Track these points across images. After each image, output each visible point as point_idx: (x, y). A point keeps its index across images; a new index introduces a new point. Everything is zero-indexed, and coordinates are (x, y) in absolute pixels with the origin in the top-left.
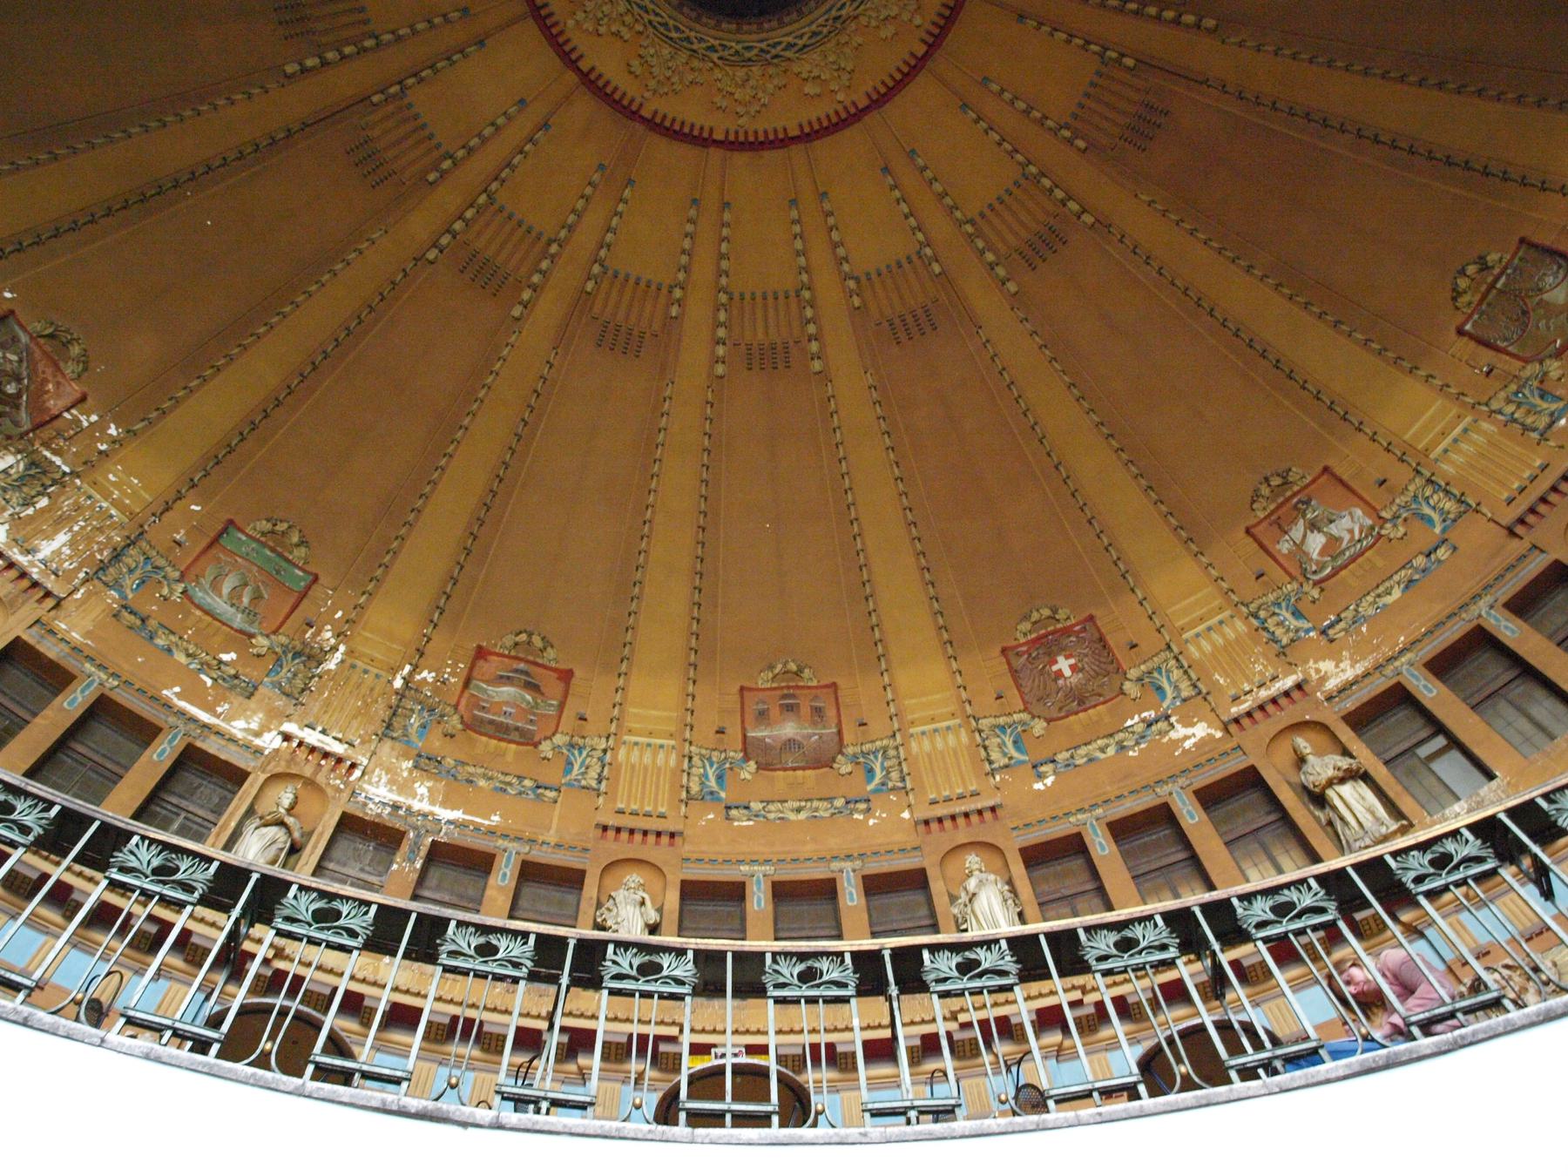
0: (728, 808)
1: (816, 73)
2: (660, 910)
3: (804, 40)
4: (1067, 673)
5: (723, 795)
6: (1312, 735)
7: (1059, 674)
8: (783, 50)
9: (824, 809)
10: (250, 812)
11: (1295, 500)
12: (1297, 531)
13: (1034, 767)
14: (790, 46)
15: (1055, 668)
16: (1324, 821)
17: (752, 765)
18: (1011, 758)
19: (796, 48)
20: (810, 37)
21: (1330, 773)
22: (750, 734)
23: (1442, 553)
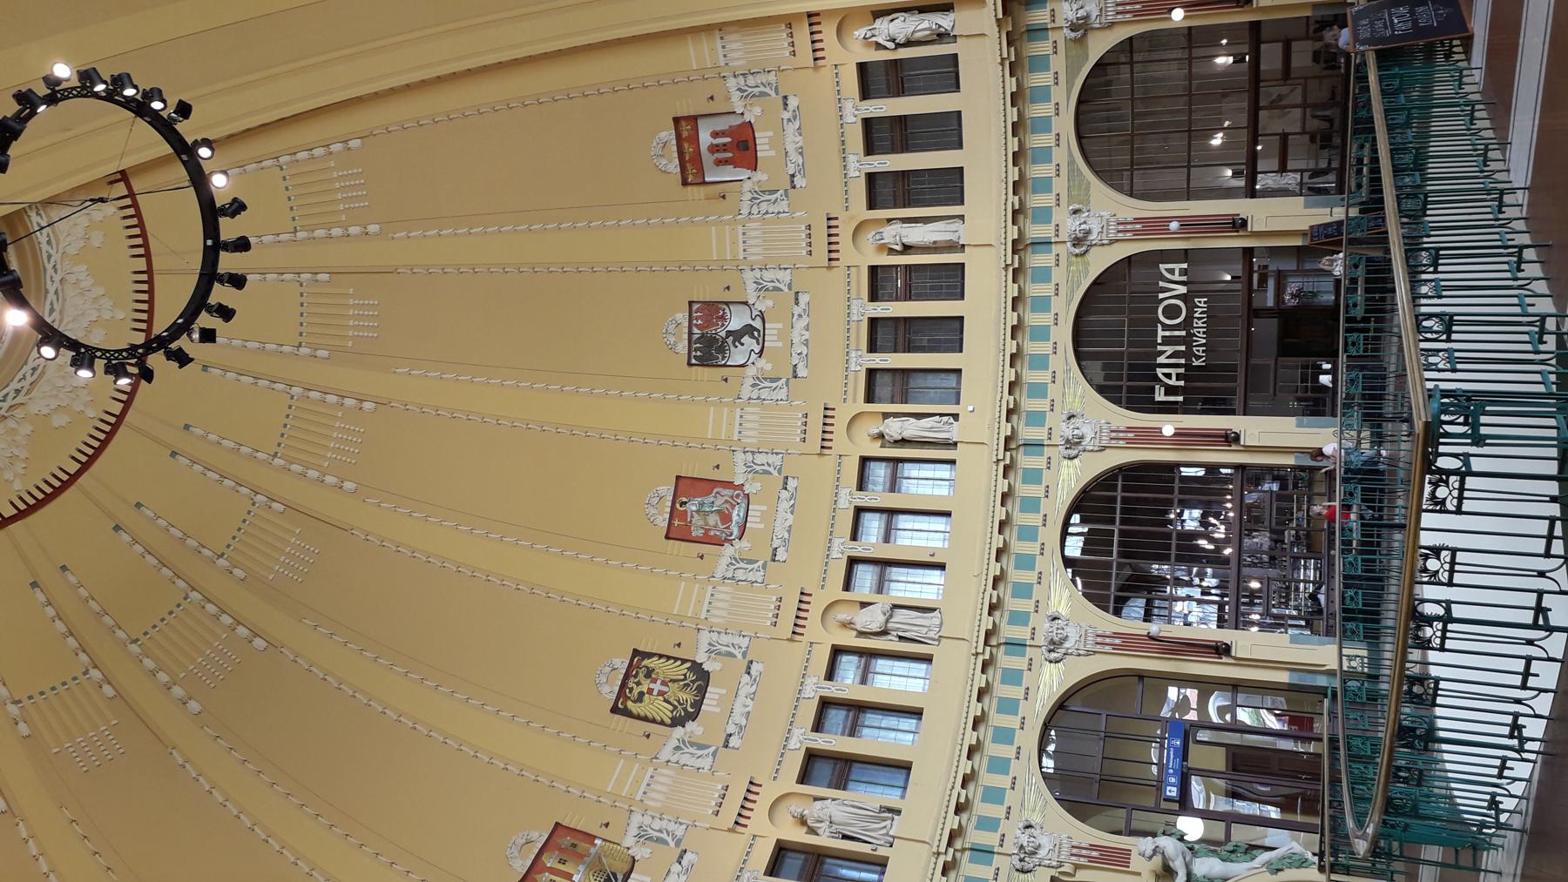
1: (54, 404)
3: (29, 379)
4: (664, 689)
6: (838, 608)
7: (661, 693)
8: (14, 398)
11: (678, 506)
12: (697, 520)
13: (727, 747)
14: (18, 391)
15: (655, 693)
16: (897, 639)
18: (707, 755)
19: (23, 392)
20: (32, 375)
21: (882, 619)
23: (792, 484)
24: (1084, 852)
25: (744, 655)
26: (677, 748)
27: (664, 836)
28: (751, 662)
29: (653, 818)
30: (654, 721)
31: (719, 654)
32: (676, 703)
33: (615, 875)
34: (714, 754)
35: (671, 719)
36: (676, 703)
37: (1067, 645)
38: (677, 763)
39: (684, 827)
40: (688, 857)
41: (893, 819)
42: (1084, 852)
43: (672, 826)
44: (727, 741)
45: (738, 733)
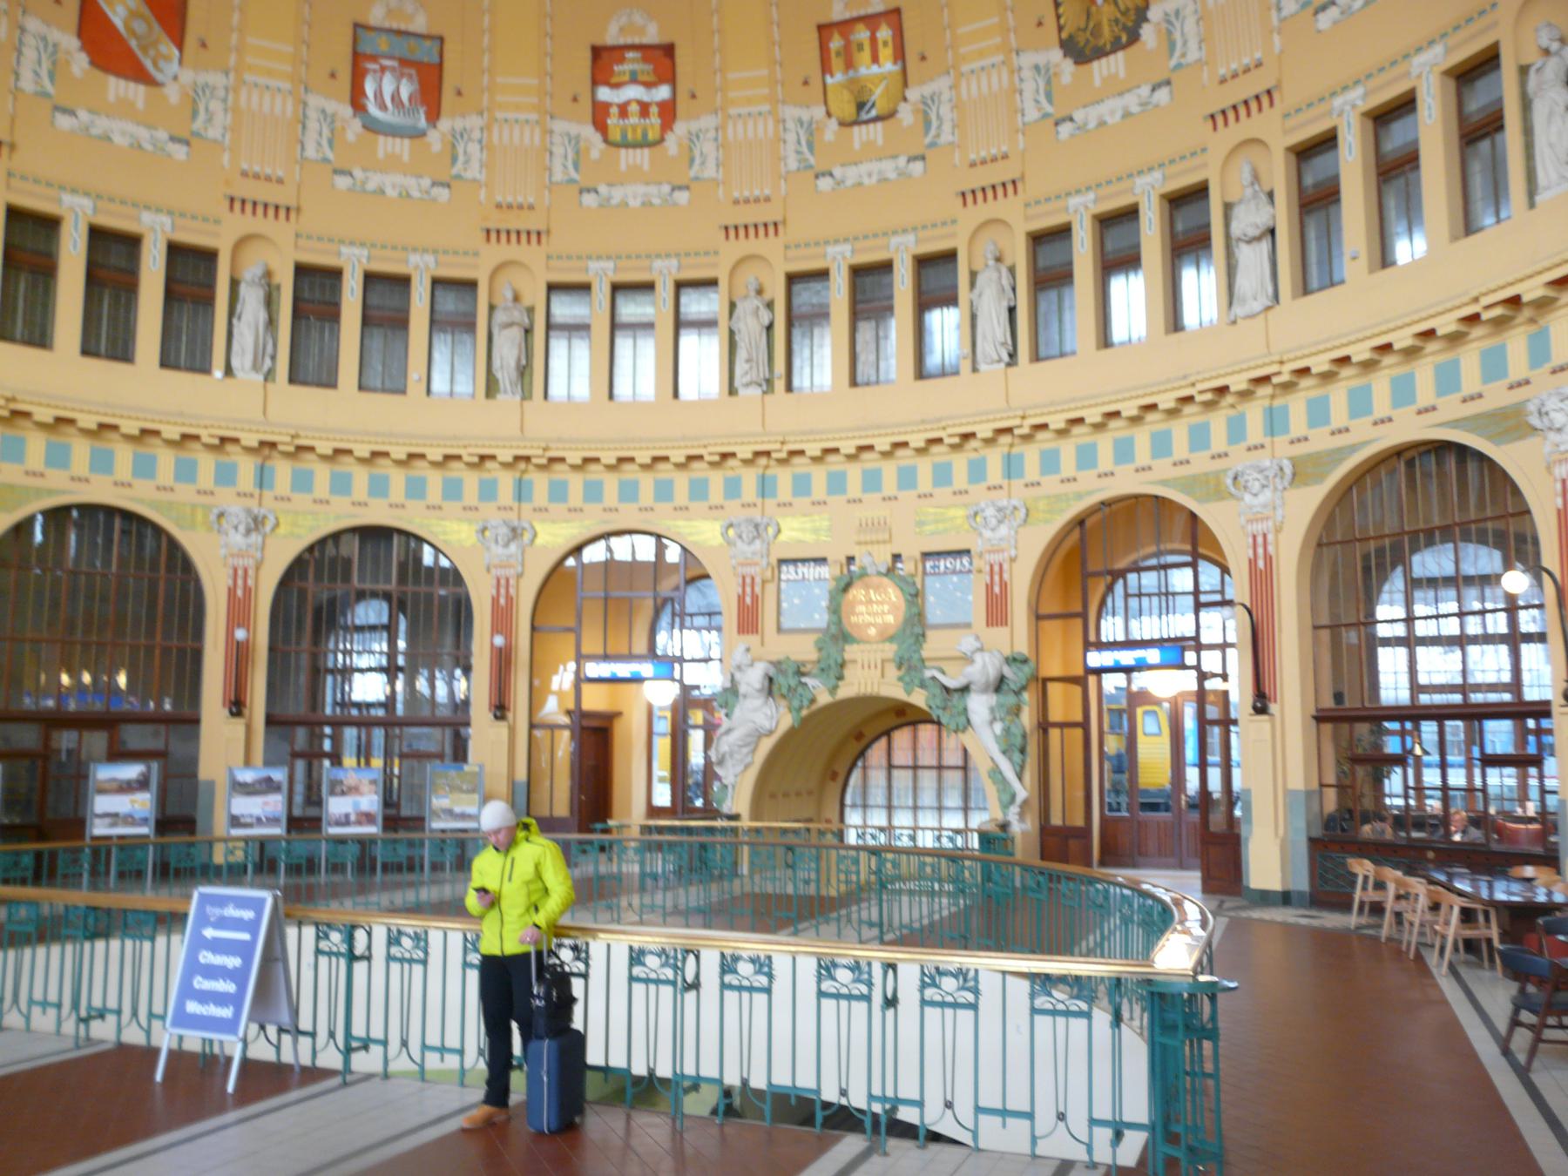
0: (817, 177)
2: (770, 305)
5: (812, 160)
9: (888, 168)
10: (492, 308)
17: (833, 124)
22: (829, 80)
24: (997, 578)
25: (1179, 66)
26: (1037, 68)
27: (935, 123)
28: (1168, 83)
29: (950, 100)
30: (1058, 17)
31: (1169, 33)
32: (1091, 25)
33: (873, 105)
34: (1046, 116)
35: (1071, 37)
36: (1091, 25)
37: (1248, 498)
38: (1021, 80)
39: (950, 138)
40: (918, 167)
41: (1000, 361)
42: (997, 578)
43: (947, 127)
44: (1063, 120)
45: (1079, 128)
